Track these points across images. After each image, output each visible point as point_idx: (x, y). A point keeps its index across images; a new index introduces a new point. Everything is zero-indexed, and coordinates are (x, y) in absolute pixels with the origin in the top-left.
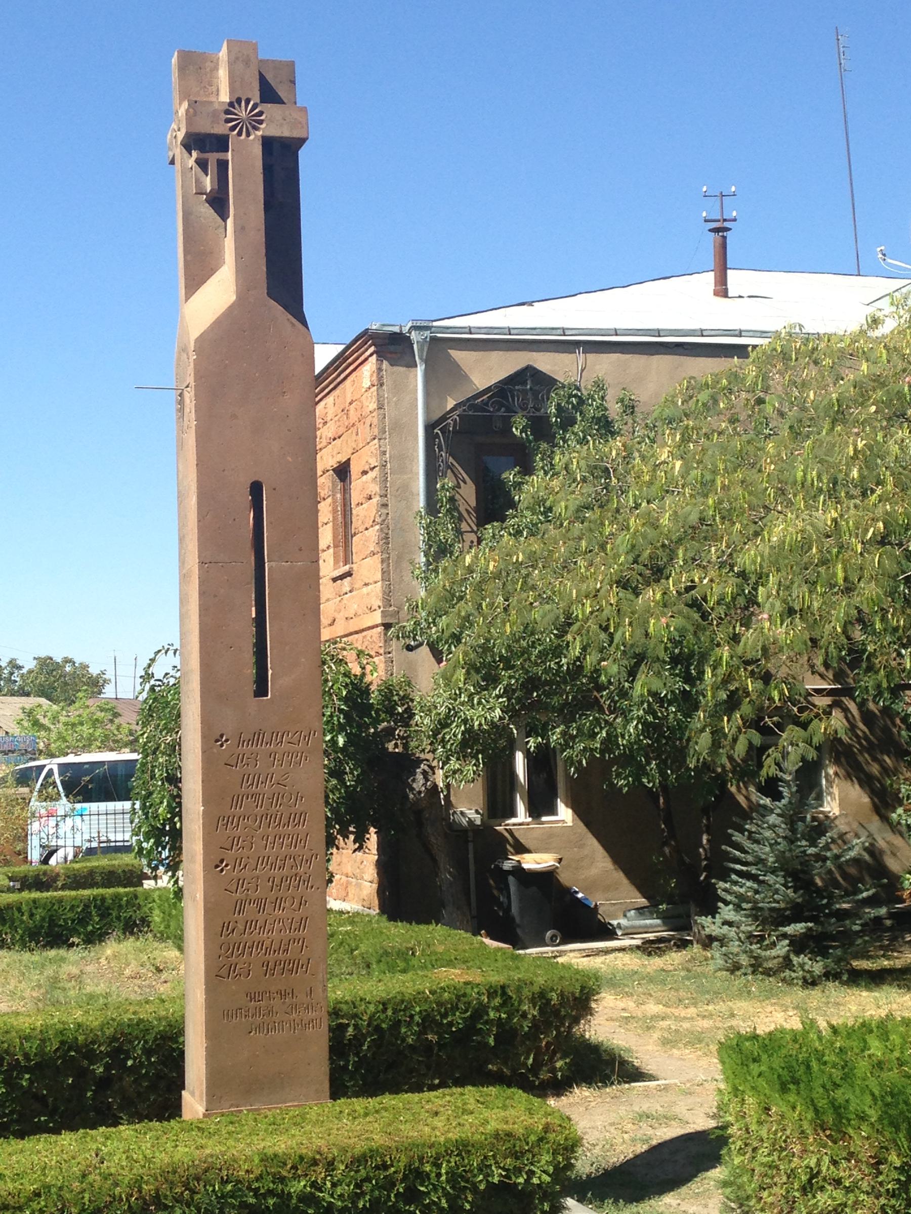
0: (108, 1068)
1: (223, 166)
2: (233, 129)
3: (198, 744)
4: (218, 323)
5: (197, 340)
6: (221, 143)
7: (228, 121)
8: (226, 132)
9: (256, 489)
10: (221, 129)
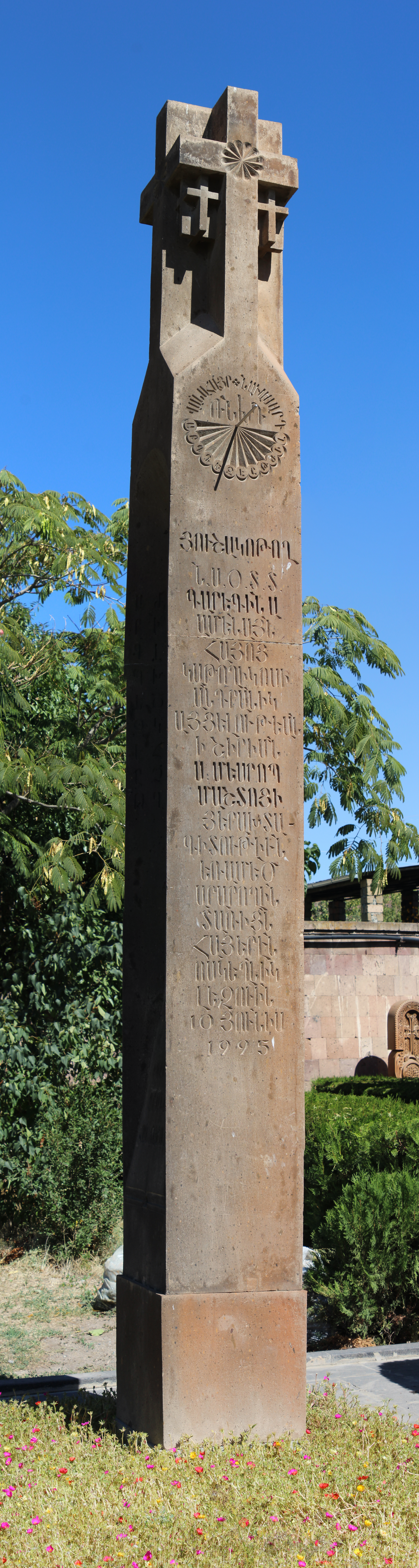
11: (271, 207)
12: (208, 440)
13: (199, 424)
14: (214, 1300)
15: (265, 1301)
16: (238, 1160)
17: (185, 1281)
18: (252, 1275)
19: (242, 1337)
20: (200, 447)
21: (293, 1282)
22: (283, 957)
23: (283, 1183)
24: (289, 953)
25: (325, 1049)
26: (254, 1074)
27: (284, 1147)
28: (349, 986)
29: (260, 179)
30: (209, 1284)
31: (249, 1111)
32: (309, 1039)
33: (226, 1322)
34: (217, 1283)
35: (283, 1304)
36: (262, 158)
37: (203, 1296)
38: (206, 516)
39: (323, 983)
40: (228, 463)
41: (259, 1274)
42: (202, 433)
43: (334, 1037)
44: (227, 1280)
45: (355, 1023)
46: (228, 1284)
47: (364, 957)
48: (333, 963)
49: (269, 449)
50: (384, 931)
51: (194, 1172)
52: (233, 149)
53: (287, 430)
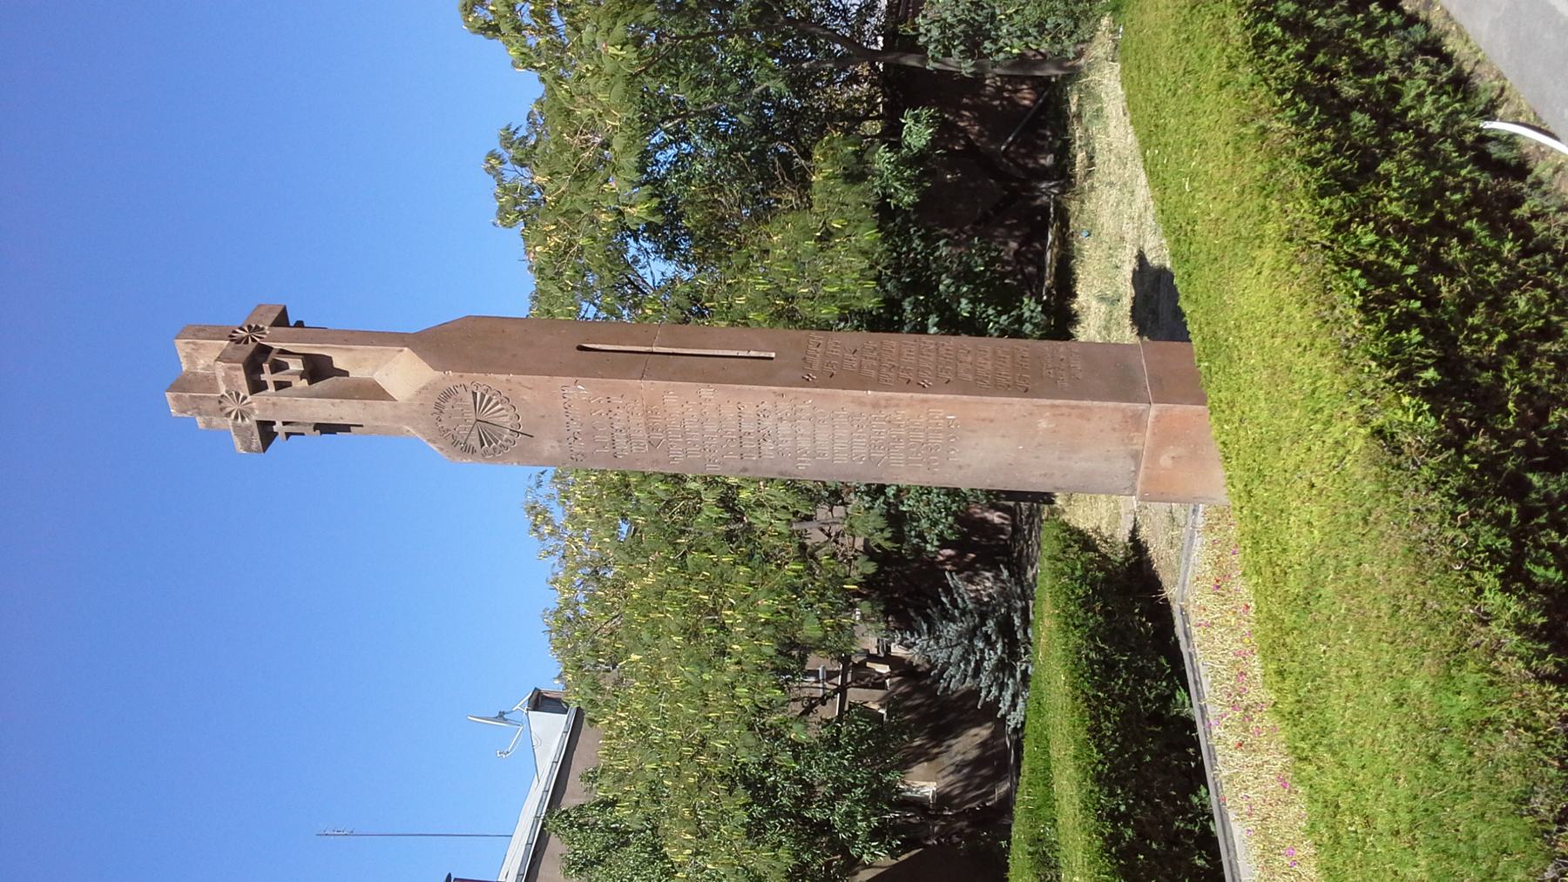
0: (1126, 825)
1: (283, 352)
2: (254, 340)
3: (809, 399)
4: (424, 358)
5: (435, 370)
6: (264, 351)
7: (247, 342)
8: (255, 344)
9: (581, 348)
10: (251, 346)
11: (267, 376)
12: (494, 439)
13: (483, 445)
14: (1146, 468)
15: (1154, 434)
16: (1040, 445)
17: (1128, 484)
18: (1132, 439)
19: (1180, 451)
20: (502, 446)
21: (1144, 410)
22: (886, 407)
23: (1062, 415)
24: (883, 403)
26: (973, 431)
27: (1030, 414)
29: (247, 394)
30: (1133, 469)
31: (1003, 436)
33: (1165, 461)
34: (1133, 464)
35: (1159, 421)
36: (227, 392)
37: (1141, 475)
38: (555, 444)
40: (508, 425)
41: (1132, 434)
42: (490, 445)
44: (1132, 457)
46: (1136, 456)
49: (487, 397)
51: (1045, 475)
52: (230, 413)
53: (468, 384)
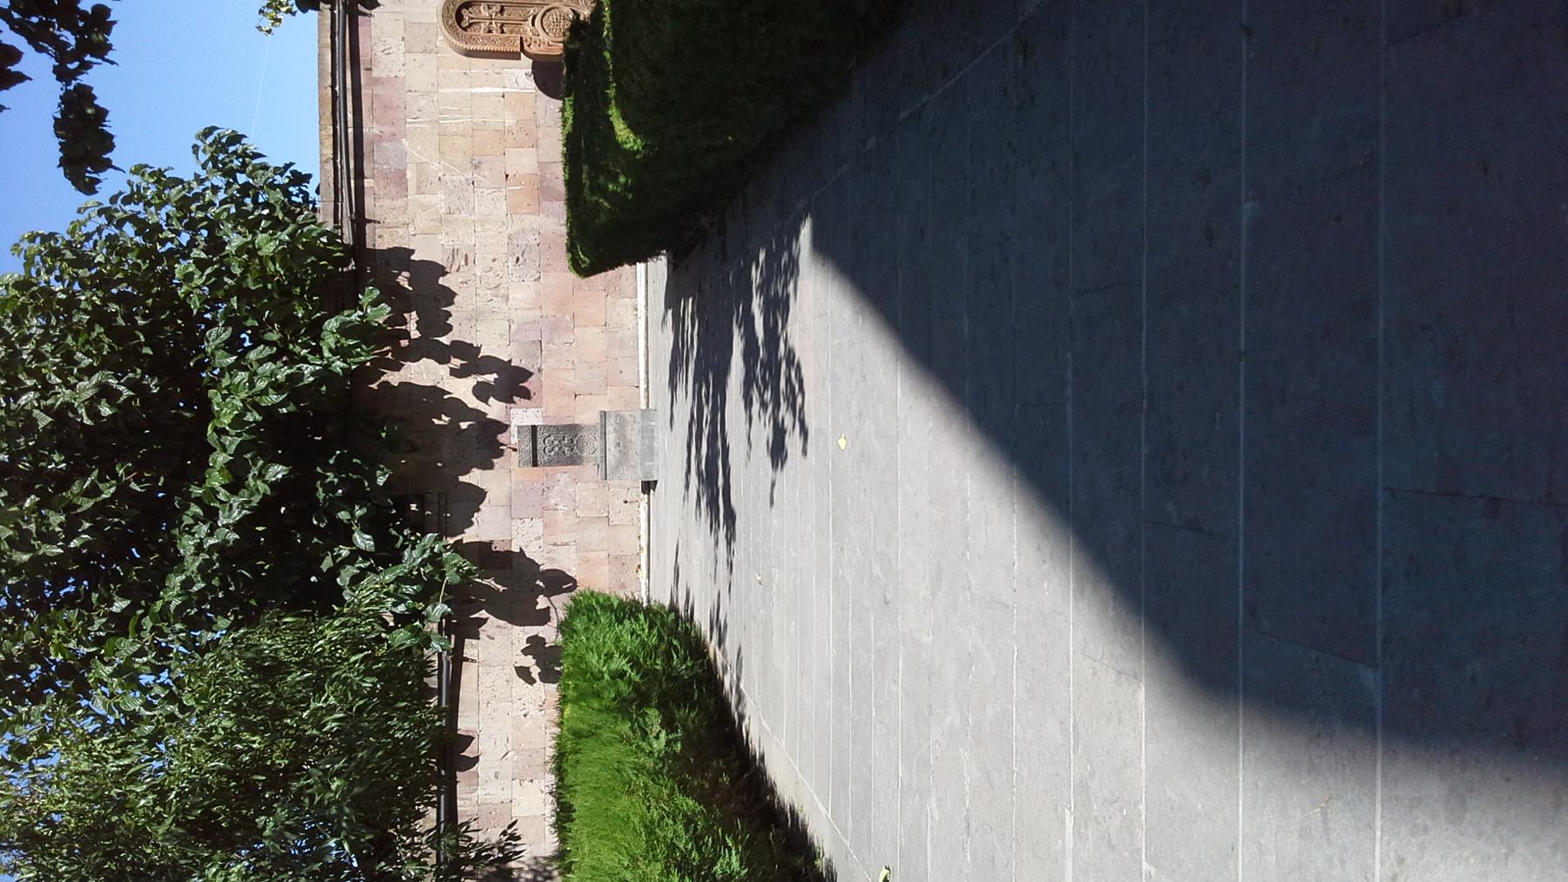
25: (522, 150)
28: (422, 102)
32: (507, 176)
39: (419, 148)
43: (503, 133)
45: (481, 95)
47: (375, 74)
48: (388, 130)
50: (333, 37)
